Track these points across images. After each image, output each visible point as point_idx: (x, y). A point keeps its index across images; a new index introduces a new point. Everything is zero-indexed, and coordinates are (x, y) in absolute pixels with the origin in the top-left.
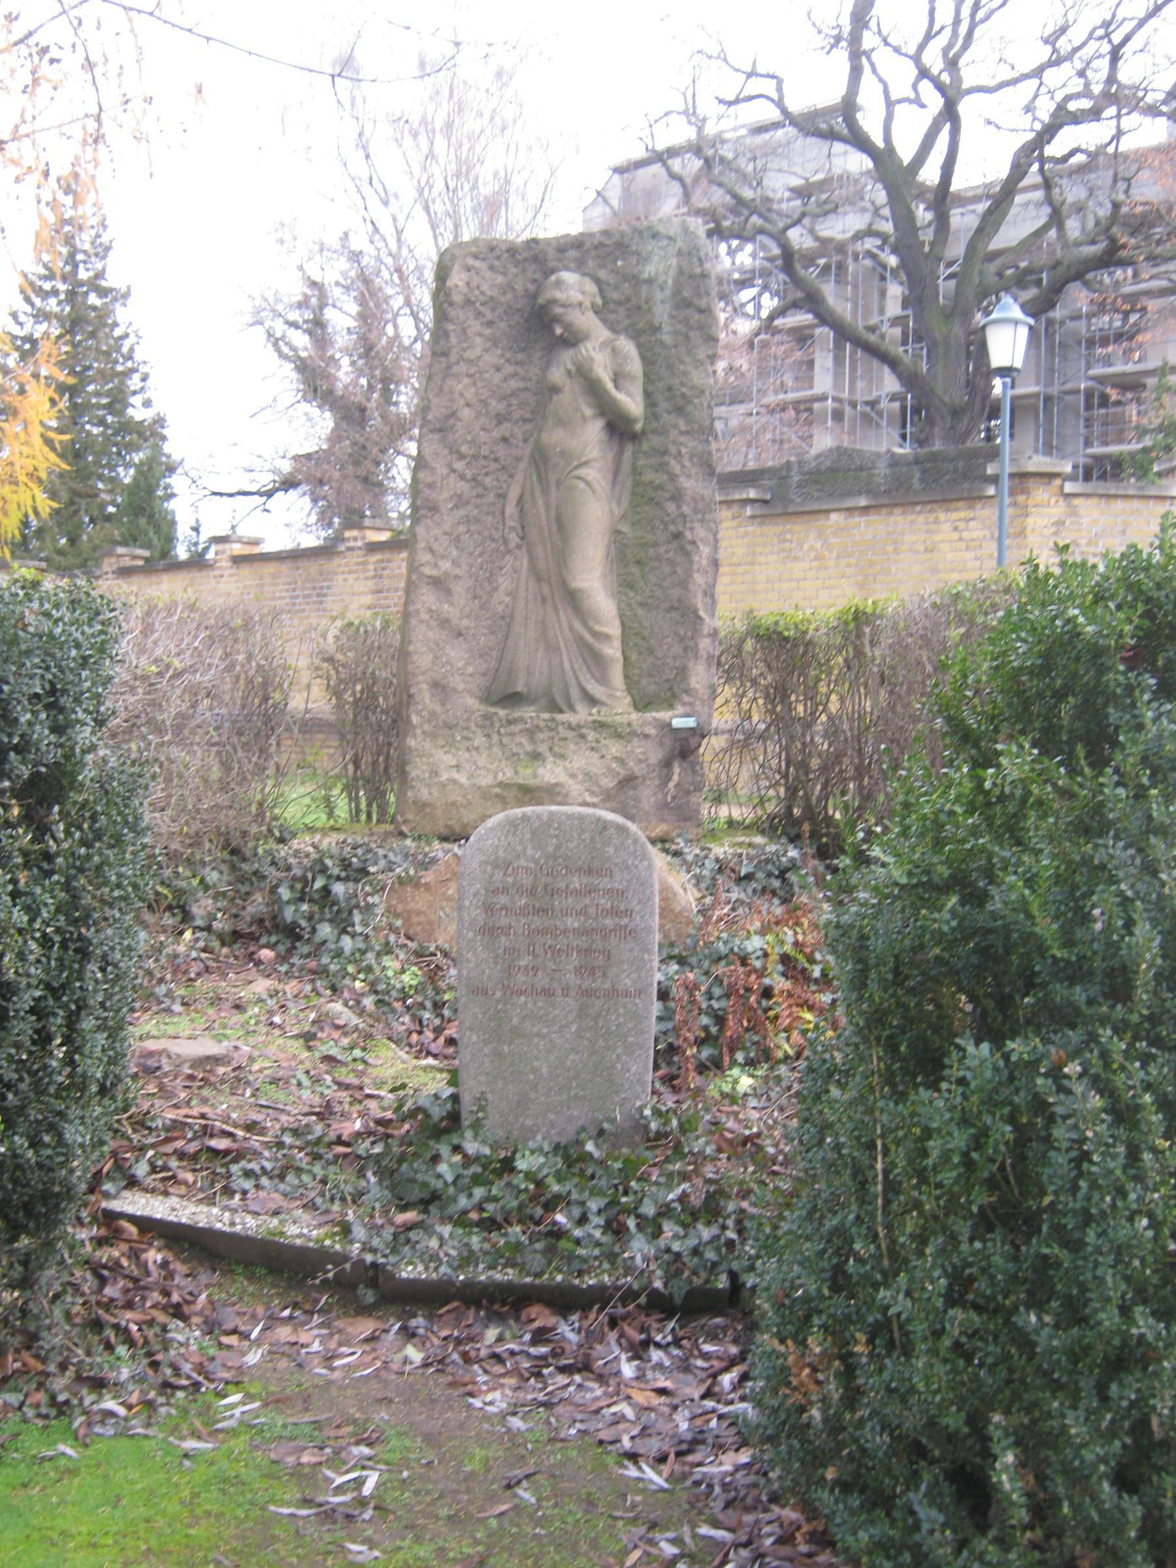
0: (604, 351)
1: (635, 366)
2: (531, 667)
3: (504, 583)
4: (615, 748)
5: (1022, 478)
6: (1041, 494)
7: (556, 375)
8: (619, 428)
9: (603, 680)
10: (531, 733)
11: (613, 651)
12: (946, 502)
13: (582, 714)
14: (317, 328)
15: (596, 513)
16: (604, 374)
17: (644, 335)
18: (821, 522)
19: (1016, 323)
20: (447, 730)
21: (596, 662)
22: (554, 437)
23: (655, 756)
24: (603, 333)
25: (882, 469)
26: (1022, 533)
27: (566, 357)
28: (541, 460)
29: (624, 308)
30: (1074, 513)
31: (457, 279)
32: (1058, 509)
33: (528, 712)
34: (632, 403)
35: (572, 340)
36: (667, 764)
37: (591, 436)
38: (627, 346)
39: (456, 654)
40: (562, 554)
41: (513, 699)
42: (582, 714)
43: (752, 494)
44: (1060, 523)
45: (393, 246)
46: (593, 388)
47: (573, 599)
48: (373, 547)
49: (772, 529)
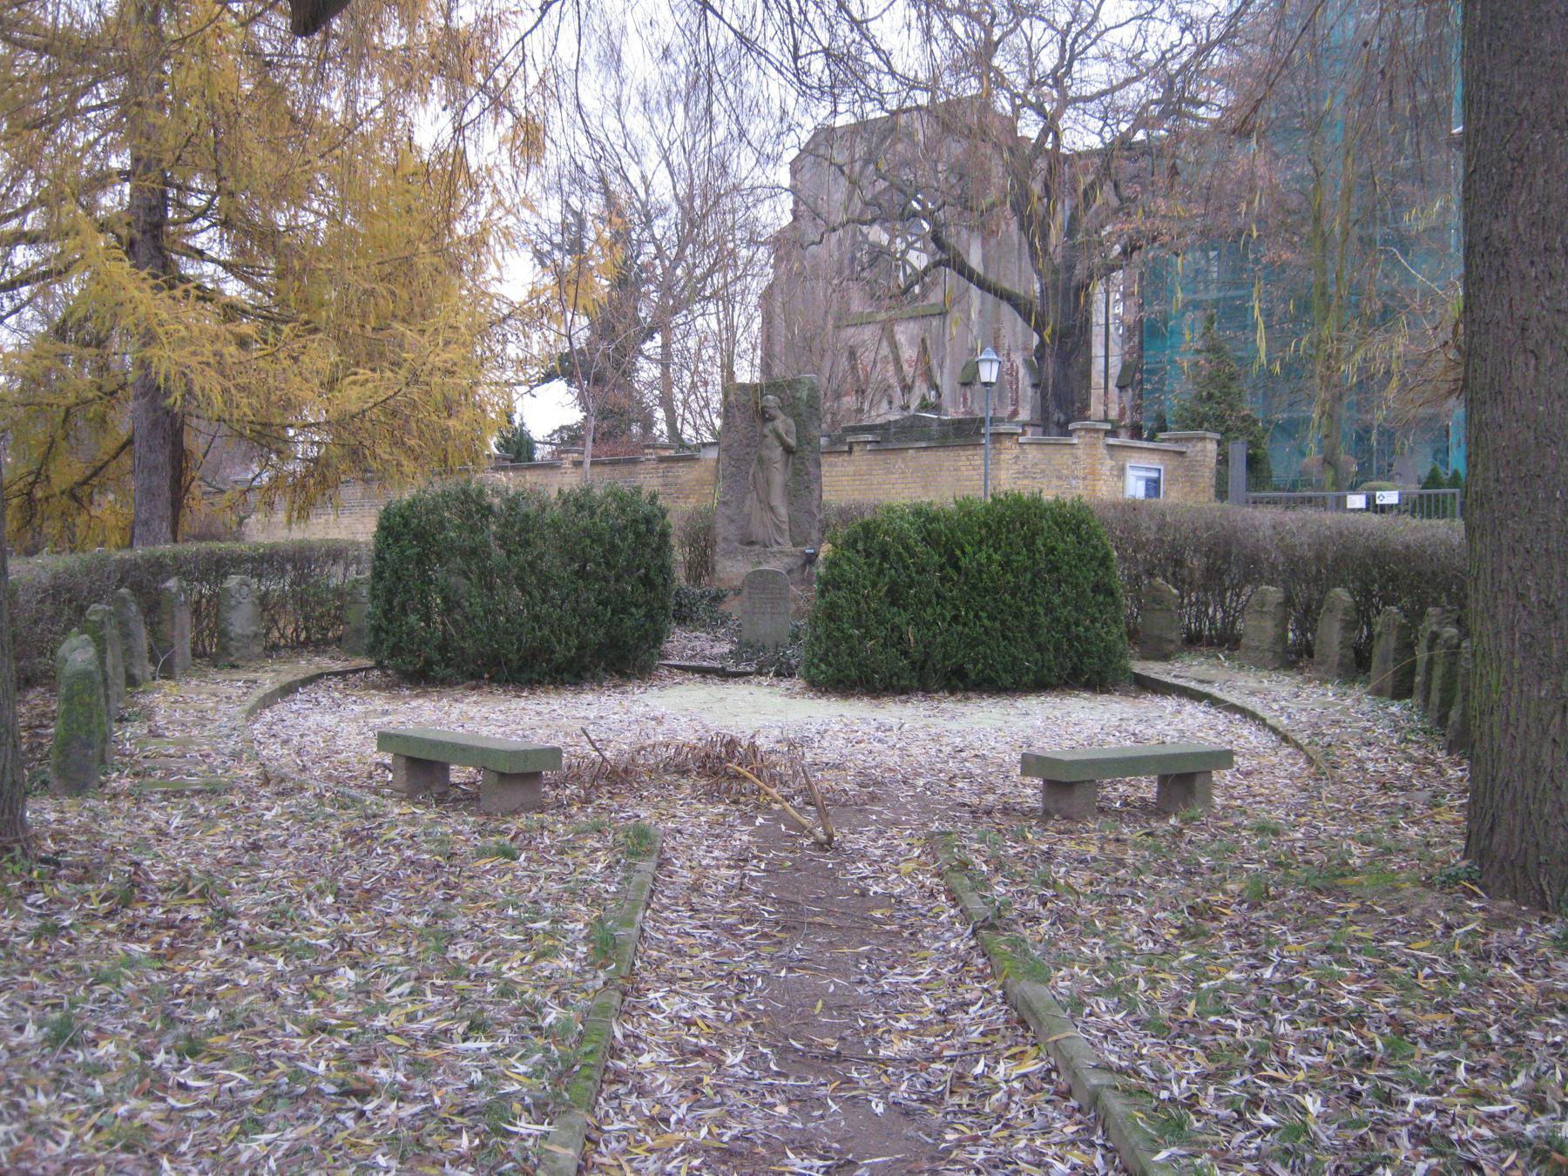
0: (783, 423)
1: (794, 429)
2: (758, 532)
3: (748, 502)
4: (786, 560)
5: (997, 436)
6: (1008, 443)
7: (766, 431)
8: (788, 450)
9: (782, 536)
10: (758, 555)
11: (785, 527)
12: (964, 446)
13: (775, 548)
14: (575, 247)
15: (779, 477)
16: (782, 431)
17: (796, 417)
18: (904, 454)
19: (991, 361)
20: (729, 554)
21: (779, 529)
22: (766, 453)
23: (800, 562)
24: (783, 417)
25: (935, 427)
26: (998, 463)
27: (770, 425)
28: (761, 460)
29: (790, 408)
30: (1024, 451)
31: (732, 398)
32: (1016, 451)
33: (757, 547)
34: (792, 441)
35: (772, 419)
36: (804, 565)
37: (777, 453)
38: (790, 421)
39: (732, 528)
40: (768, 495)
41: (752, 543)
42: (775, 548)
43: (870, 438)
44: (1017, 457)
45: (642, 195)
46: (779, 437)
47: (772, 509)
48: (662, 460)
49: (880, 457)
